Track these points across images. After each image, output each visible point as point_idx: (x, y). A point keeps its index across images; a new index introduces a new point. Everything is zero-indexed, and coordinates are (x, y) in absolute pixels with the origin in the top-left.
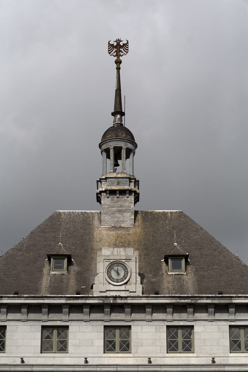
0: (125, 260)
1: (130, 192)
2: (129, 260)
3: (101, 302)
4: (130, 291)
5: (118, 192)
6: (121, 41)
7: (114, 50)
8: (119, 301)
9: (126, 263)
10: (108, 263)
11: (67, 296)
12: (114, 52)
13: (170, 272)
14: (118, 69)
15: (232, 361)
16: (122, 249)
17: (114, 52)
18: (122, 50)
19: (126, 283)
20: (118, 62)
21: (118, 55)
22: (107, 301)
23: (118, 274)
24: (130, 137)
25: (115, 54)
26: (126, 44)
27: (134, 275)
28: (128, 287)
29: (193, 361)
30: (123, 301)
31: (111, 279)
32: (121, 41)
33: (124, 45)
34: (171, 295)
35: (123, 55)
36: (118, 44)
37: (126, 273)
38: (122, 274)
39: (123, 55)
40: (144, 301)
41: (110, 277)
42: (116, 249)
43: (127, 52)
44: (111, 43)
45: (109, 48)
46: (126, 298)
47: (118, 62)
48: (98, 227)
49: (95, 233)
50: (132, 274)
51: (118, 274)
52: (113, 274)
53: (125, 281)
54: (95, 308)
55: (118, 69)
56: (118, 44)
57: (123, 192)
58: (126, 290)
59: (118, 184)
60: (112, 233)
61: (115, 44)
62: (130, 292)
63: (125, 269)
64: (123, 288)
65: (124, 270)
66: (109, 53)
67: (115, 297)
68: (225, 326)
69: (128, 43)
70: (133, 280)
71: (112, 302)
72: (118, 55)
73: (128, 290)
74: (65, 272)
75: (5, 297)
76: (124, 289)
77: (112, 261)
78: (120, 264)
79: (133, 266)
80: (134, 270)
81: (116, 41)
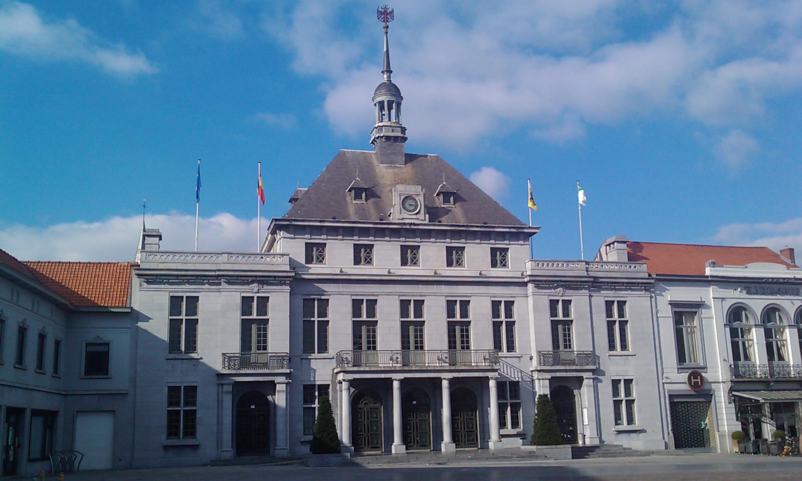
8: (413, 227)
16: (412, 186)
19: (417, 214)
22: (405, 227)
28: (418, 216)
30: (416, 227)
41: (404, 208)
42: (408, 186)
46: (419, 225)
48: (378, 166)
49: (377, 170)
52: (407, 205)
60: (389, 170)
62: (418, 219)
64: (415, 217)
67: (411, 224)
74: (364, 202)
75: (328, 221)
79: (420, 199)
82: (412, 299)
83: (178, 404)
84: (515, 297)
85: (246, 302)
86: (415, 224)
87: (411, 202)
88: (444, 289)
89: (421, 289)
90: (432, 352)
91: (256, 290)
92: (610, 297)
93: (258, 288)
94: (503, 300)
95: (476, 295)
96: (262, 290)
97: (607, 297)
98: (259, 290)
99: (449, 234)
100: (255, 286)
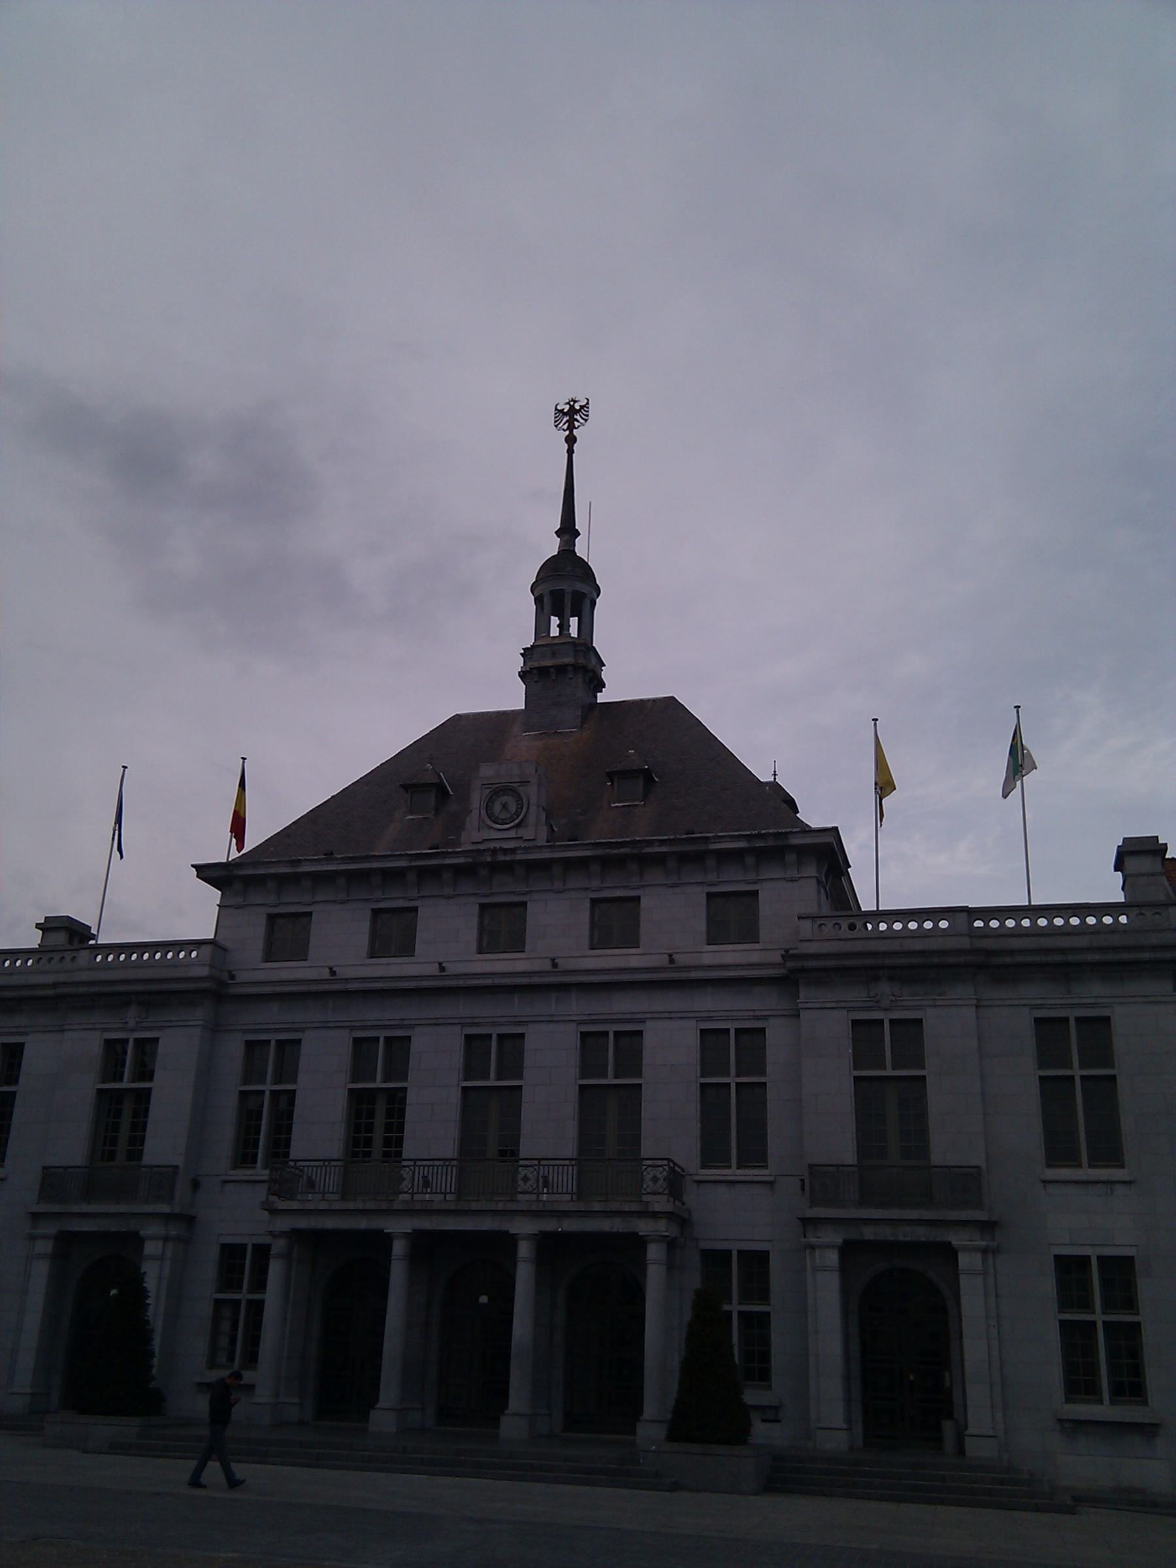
0: (518, 784)
1: (576, 668)
2: (525, 783)
3: (470, 860)
4: (525, 838)
5: (552, 670)
6: (575, 402)
7: (565, 420)
8: (501, 858)
9: (521, 788)
10: (488, 791)
11: (410, 852)
12: (564, 424)
13: (614, 803)
14: (570, 452)
15: (707, 959)
17: (564, 424)
18: (578, 417)
19: (518, 826)
20: (571, 440)
21: (571, 428)
23: (505, 806)
24: (585, 572)
25: (565, 427)
26: (585, 406)
27: (533, 809)
28: (522, 832)
29: (634, 962)
30: (508, 858)
31: (493, 819)
32: (575, 402)
33: (582, 407)
34: (593, 841)
35: (579, 426)
36: (572, 407)
37: (519, 806)
38: (513, 808)
39: (579, 426)
40: (547, 855)
43: (586, 420)
44: (559, 408)
45: (555, 418)
46: (513, 851)
47: (571, 440)
50: (531, 807)
51: (505, 806)
52: (497, 808)
53: (516, 821)
54: (464, 872)
55: (570, 452)
56: (572, 407)
57: (561, 670)
58: (518, 836)
59: (554, 655)
61: (567, 408)
63: (519, 799)
64: (512, 834)
65: (517, 801)
66: (556, 426)
67: (494, 851)
68: (698, 896)
69: (588, 403)
70: (532, 819)
71: (489, 859)
72: (571, 428)
73: (522, 838)
76: (515, 836)
77: (495, 786)
78: (510, 791)
80: (533, 800)
81: (568, 403)
82: (495, 1031)
83: (249, 1302)
84: (765, 1018)
85: (114, 1050)
86: (505, 851)
87: (510, 800)
88: (577, 1006)
89: (518, 1007)
90: (551, 1162)
91: (132, 1023)
92: (1052, 1007)
93: (138, 1019)
94: (732, 1026)
95: (656, 1017)
96: (144, 1025)
97: (1038, 1007)
98: (137, 1022)
99: (595, 868)
100: (132, 1015)
